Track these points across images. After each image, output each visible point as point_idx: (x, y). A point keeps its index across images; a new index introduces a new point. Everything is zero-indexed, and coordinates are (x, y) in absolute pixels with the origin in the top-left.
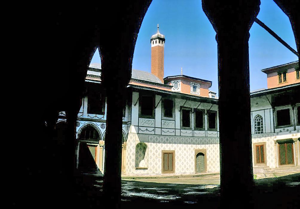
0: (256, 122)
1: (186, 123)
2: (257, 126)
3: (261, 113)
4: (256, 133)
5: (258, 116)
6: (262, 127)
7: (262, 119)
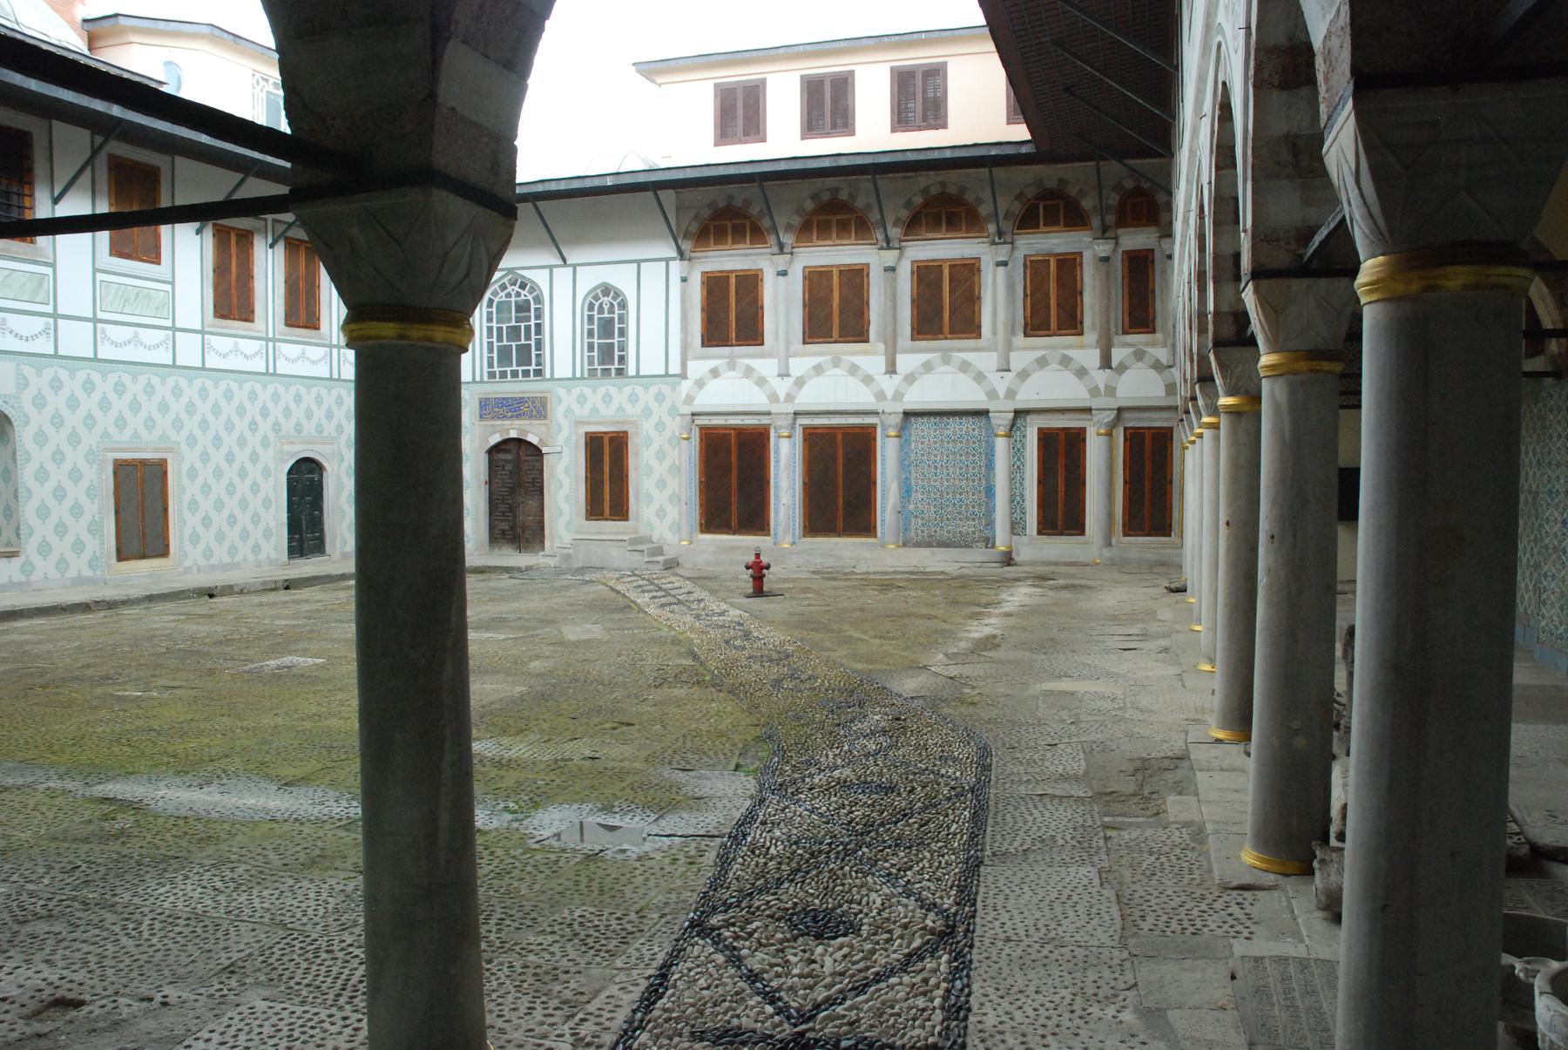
1: (233, 300)
2: (596, 341)
3: (622, 279)
5: (607, 289)
7: (623, 305)
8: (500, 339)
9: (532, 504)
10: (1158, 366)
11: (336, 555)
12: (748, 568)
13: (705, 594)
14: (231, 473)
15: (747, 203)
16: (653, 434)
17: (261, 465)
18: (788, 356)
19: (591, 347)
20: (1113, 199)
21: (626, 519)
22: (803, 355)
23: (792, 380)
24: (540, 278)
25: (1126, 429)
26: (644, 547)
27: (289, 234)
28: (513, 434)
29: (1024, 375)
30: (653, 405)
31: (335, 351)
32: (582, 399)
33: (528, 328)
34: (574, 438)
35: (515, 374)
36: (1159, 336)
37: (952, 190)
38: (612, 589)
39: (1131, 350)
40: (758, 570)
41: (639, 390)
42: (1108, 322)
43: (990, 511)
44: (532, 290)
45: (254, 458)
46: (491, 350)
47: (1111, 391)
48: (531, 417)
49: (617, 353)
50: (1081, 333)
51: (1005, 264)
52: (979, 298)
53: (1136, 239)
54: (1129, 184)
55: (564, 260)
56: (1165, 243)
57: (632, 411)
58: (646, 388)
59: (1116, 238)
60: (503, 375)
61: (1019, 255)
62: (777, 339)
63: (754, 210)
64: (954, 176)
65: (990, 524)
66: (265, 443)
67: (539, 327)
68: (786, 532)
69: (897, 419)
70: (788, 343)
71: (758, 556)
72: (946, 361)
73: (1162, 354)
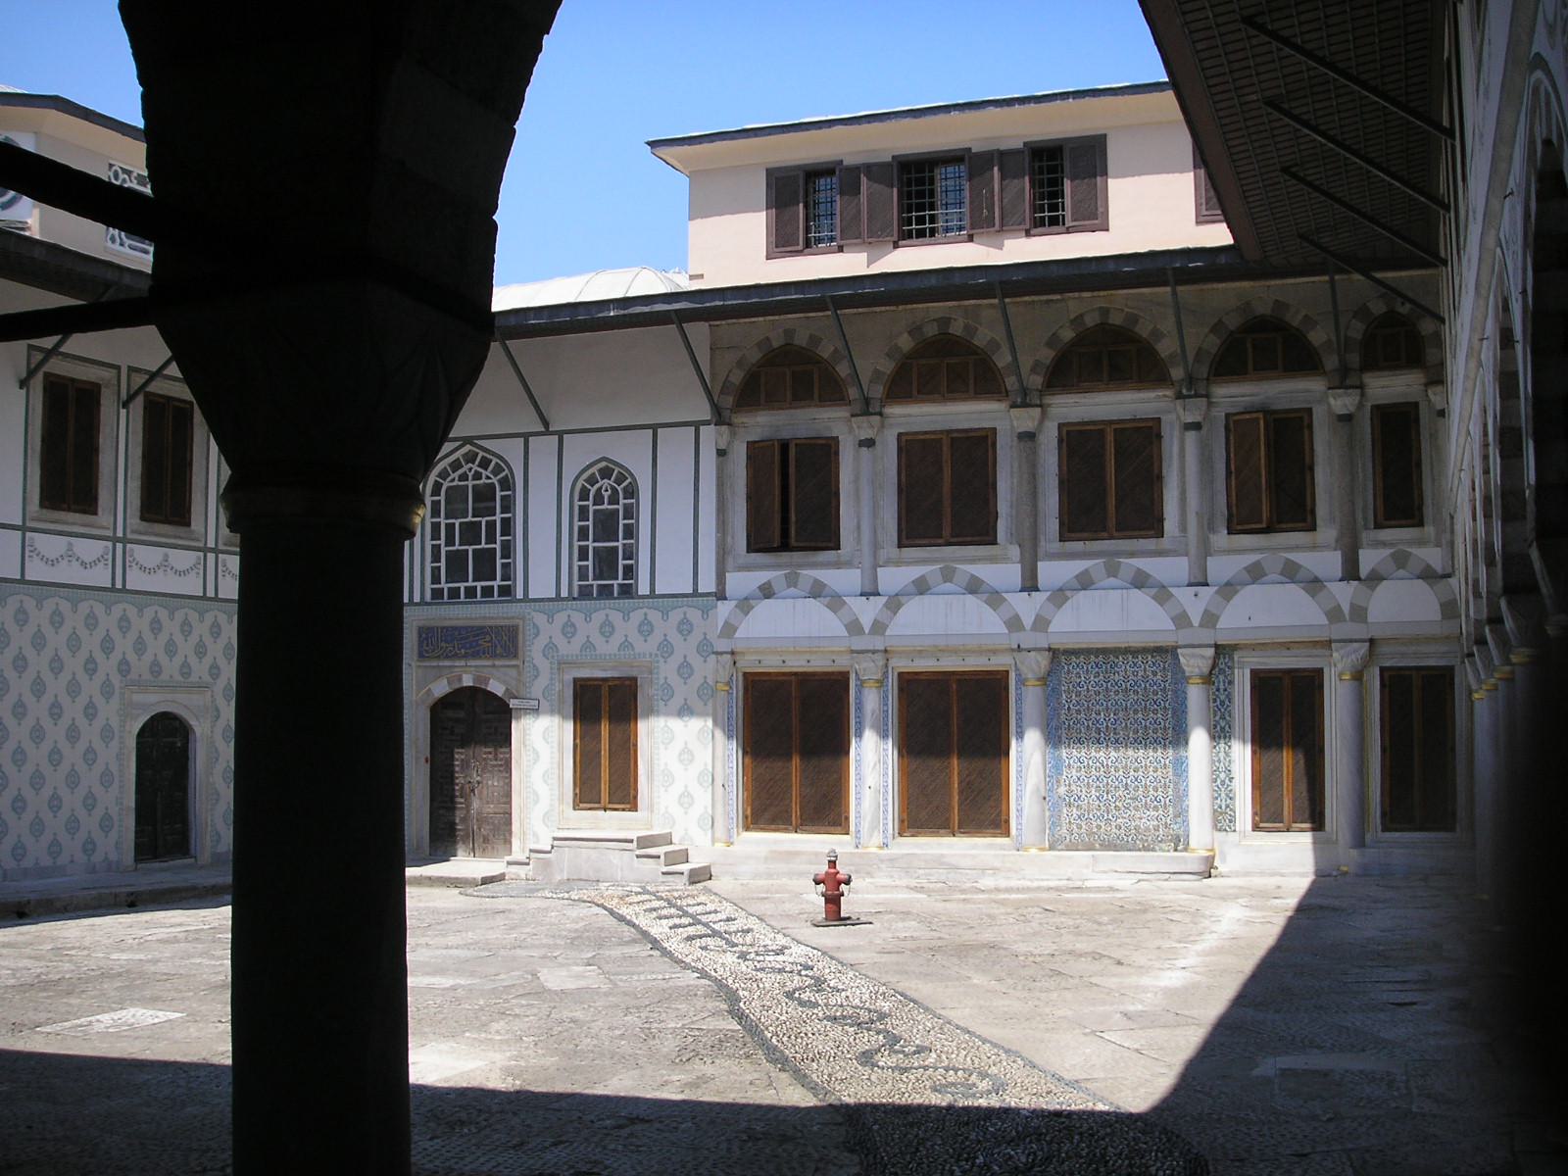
0: (583, 511)
2: (591, 544)
3: (630, 452)
4: (585, 593)
6: (630, 553)
7: (632, 492)
8: (450, 541)
9: (494, 782)
10: (1428, 575)
11: (205, 857)
12: (817, 883)
13: (752, 922)
14: (56, 733)
15: (815, 340)
16: (675, 680)
17: (98, 723)
18: (875, 566)
19: (583, 554)
20: (1357, 330)
21: (634, 808)
22: (898, 563)
23: (884, 599)
24: (511, 451)
25: (1382, 670)
26: (660, 850)
27: (151, 388)
28: (467, 681)
29: (1229, 589)
30: (675, 638)
31: (211, 556)
32: (569, 630)
33: (491, 525)
34: (557, 687)
35: (471, 592)
36: (1429, 530)
37: (1116, 319)
38: (612, 912)
39: (1386, 552)
40: (833, 887)
41: (654, 616)
42: (1353, 513)
43: (1181, 797)
44: (498, 470)
45: (91, 711)
46: (436, 558)
47: (1359, 613)
48: (494, 656)
49: (621, 563)
50: (1313, 528)
51: (1196, 426)
52: (1160, 478)
53: (1391, 386)
54: (1378, 308)
55: (546, 424)
56: (1435, 396)
57: (645, 647)
58: (665, 614)
59: (1361, 387)
60: (454, 593)
61: (1219, 414)
62: (859, 540)
63: (826, 351)
64: (1122, 300)
65: (1181, 814)
66: (107, 691)
67: (507, 526)
68: (874, 828)
69: (1043, 661)
70: (876, 546)
71: (832, 864)
72: (1112, 571)
73: (1433, 556)
